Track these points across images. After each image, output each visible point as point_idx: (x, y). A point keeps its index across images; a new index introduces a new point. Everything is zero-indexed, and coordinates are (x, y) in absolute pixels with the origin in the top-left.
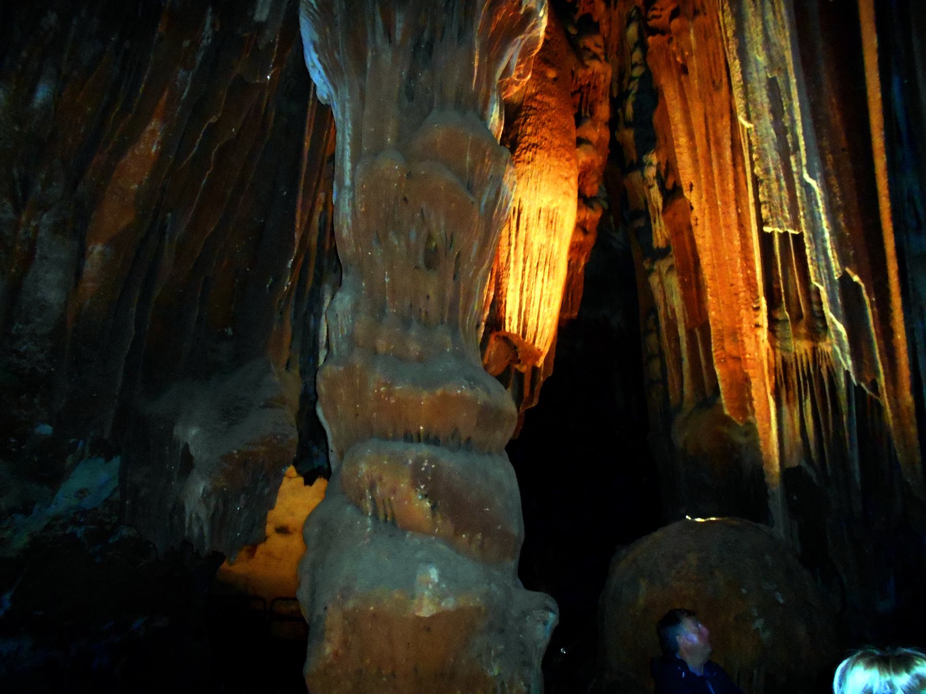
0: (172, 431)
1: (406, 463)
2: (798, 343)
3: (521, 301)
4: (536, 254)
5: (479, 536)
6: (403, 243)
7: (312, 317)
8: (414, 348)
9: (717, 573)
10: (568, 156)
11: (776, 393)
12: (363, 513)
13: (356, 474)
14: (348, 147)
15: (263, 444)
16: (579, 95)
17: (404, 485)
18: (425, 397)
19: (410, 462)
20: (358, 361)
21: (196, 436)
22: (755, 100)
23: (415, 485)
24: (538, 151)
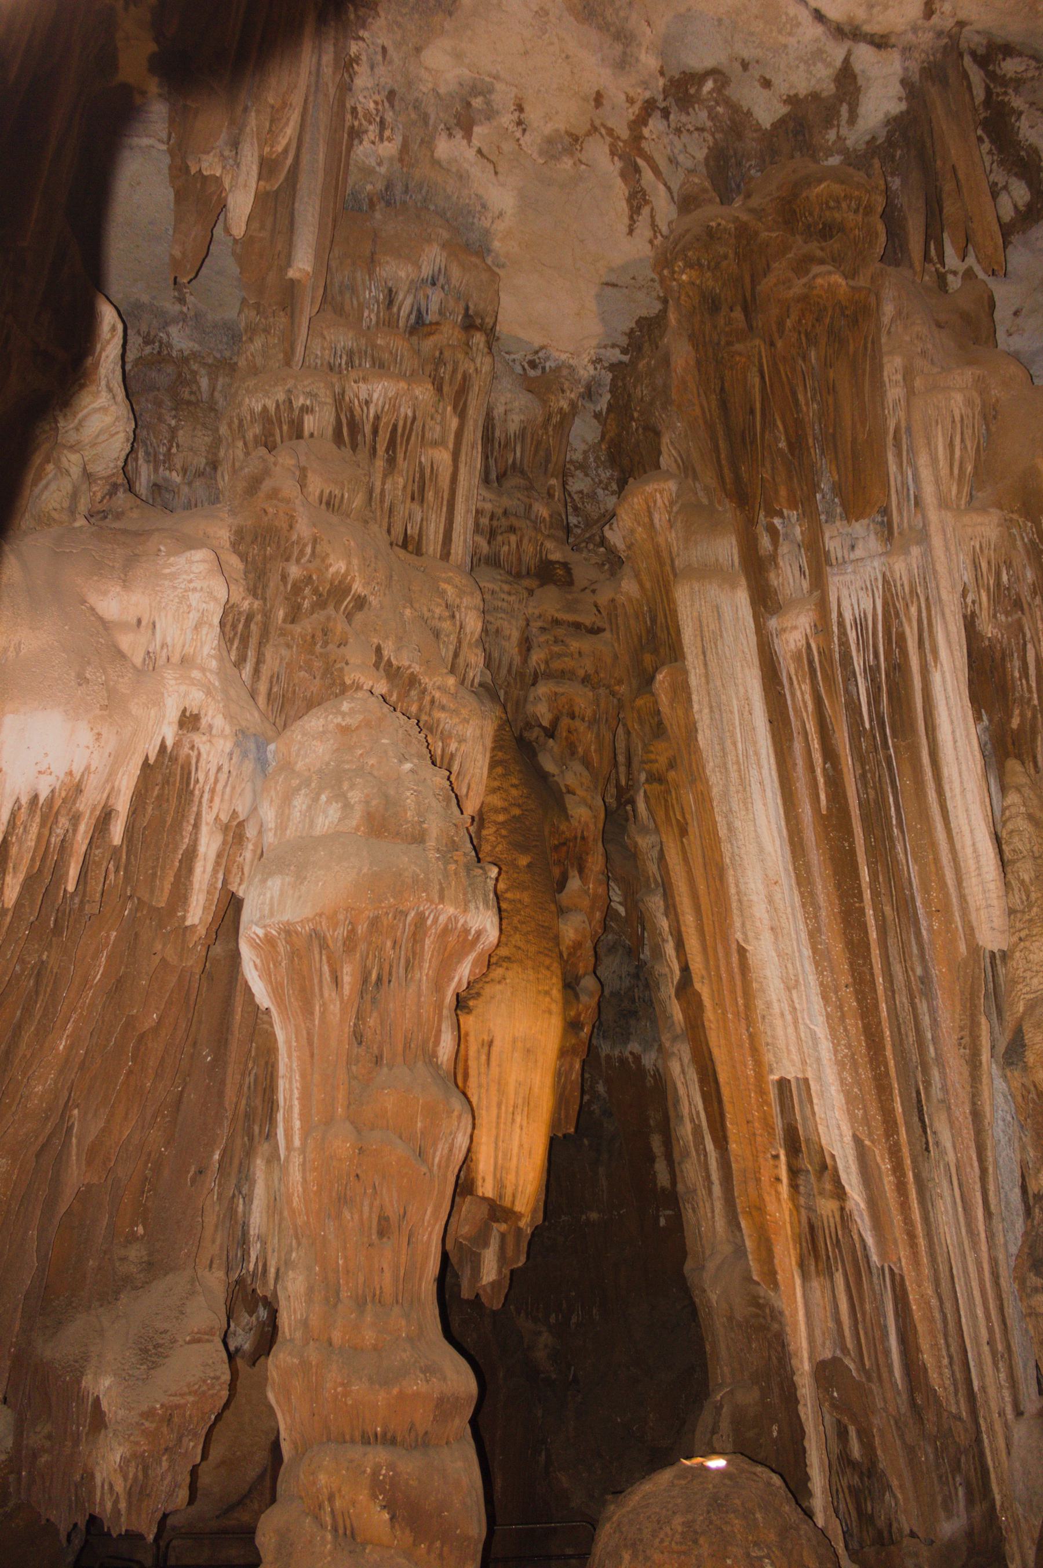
0: (79, 1382)
1: (365, 1472)
2: (823, 1201)
3: (496, 1157)
4: (512, 1095)
5: (438, 1544)
6: (356, 1216)
7: (241, 1201)
8: (369, 1336)
9: (701, 1540)
10: (548, 962)
11: (801, 1265)
12: (322, 1526)
13: (314, 1483)
14: (296, 1102)
15: (190, 1393)
16: (565, 848)
17: (363, 1497)
18: (381, 1397)
19: (369, 1470)
20: (313, 1355)
21: (109, 1388)
22: (752, 916)
23: (374, 1497)
24: (510, 965)
